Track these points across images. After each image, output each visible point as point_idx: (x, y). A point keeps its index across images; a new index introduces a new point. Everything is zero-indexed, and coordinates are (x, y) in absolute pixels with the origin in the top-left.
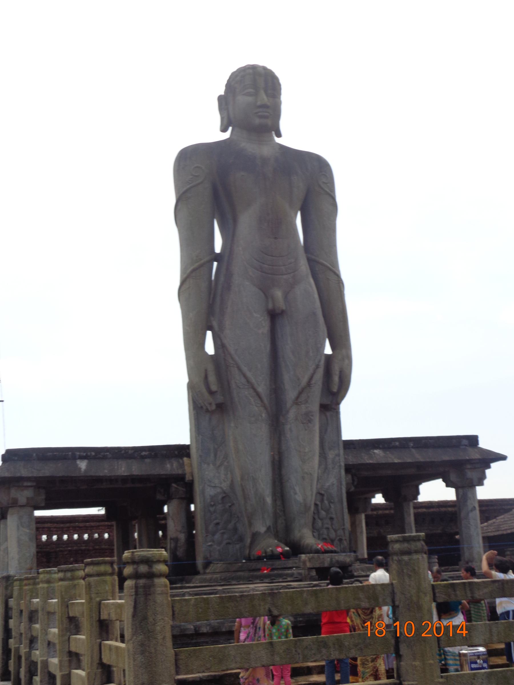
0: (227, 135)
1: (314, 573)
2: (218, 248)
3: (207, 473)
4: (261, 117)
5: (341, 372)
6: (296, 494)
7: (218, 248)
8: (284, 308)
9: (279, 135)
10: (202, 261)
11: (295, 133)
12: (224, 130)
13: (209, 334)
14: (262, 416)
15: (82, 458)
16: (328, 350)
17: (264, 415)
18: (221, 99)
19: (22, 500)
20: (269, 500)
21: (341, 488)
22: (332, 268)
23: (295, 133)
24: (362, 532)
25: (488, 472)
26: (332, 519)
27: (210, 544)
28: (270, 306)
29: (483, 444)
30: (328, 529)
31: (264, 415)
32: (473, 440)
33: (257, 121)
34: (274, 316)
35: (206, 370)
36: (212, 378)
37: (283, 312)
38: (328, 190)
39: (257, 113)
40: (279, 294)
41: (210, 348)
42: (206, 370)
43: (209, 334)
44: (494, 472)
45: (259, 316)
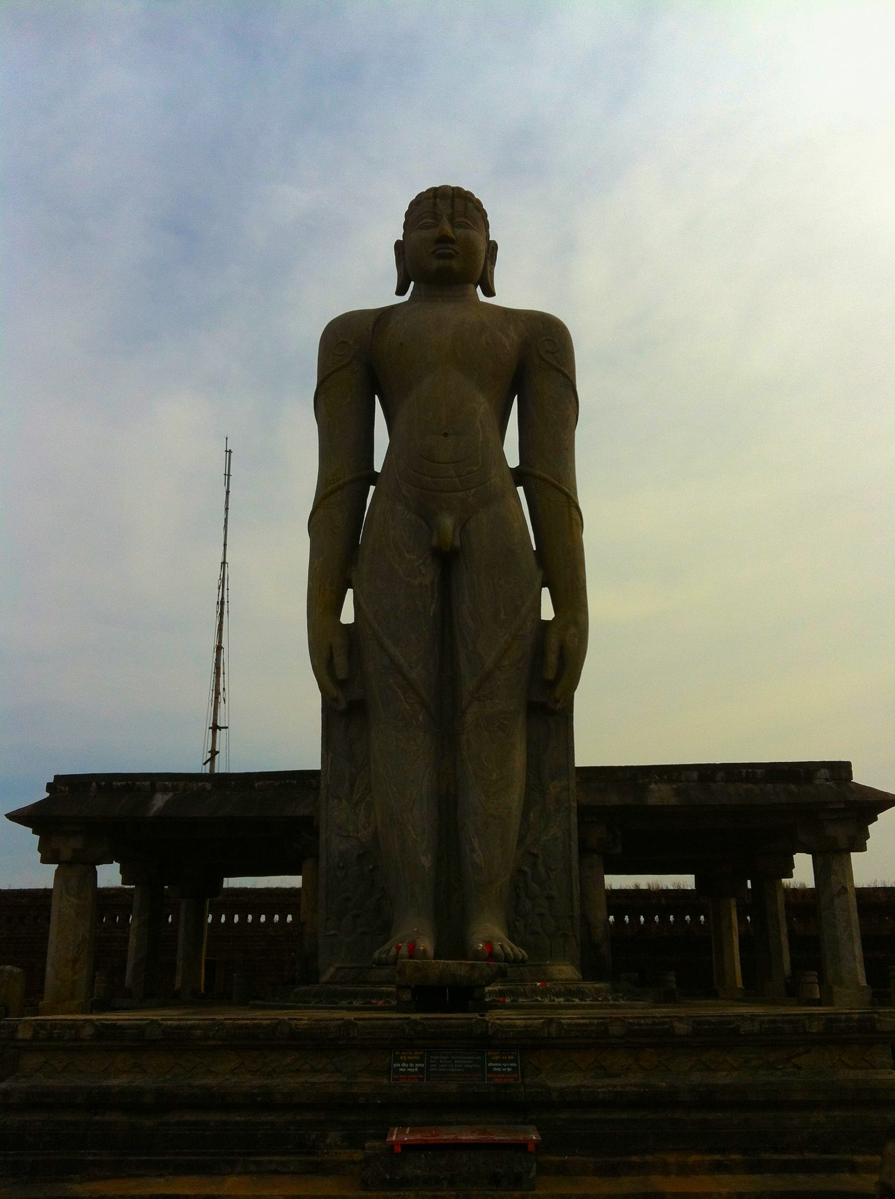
0: (406, 298)
1: (407, 996)
3: (336, 813)
4: (441, 257)
5: (562, 648)
6: (473, 851)
8: (457, 543)
10: (341, 482)
11: (516, 286)
12: (401, 291)
13: (350, 593)
14: (418, 720)
15: (165, 790)
16: (547, 612)
17: (421, 718)
18: (399, 246)
20: (426, 861)
21: (570, 845)
22: (557, 483)
23: (516, 286)
24: (730, 927)
25: (871, 827)
26: (550, 898)
27: (332, 932)
28: (434, 541)
29: (858, 778)
30: (541, 915)
31: (421, 718)
33: (436, 264)
35: (331, 647)
36: (340, 661)
38: (555, 363)
39: (433, 253)
40: (448, 522)
41: (348, 615)
42: (331, 647)
44: (885, 827)
45: (414, 557)
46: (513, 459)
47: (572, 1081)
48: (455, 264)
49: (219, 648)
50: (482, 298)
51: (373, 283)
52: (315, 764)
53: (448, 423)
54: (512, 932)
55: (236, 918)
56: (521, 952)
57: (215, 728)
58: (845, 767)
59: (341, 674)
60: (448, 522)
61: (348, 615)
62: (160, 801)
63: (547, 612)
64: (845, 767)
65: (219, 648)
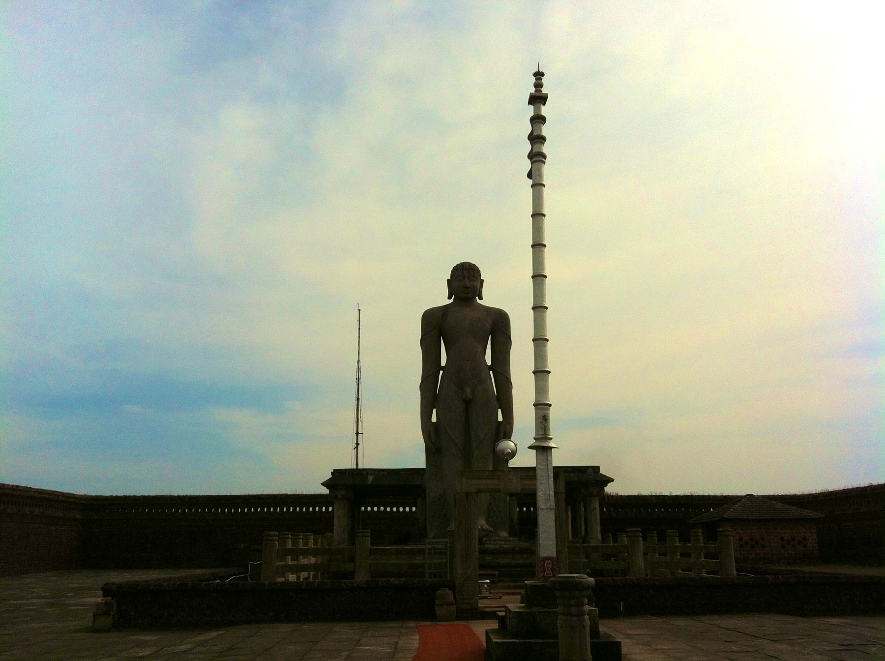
0: (451, 301)
2: (443, 362)
7: (443, 363)
9: (481, 298)
11: (490, 298)
12: (450, 298)
13: (435, 410)
15: (371, 474)
16: (500, 419)
19: (340, 496)
23: (490, 298)
29: (602, 471)
32: (597, 469)
33: (463, 295)
34: (467, 403)
37: (471, 400)
40: (468, 391)
41: (434, 419)
43: (435, 410)
46: (489, 363)
47: (506, 561)
48: (470, 295)
49: (358, 399)
50: (478, 301)
51: (441, 298)
52: (423, 465)
53: (464, 337)
54: (488, 522)
55: (311, 509)
56: (491, 529)
57: (357, 433)
58: (598, 468)
59: (433, 440)
60: (468, 391)
61: (434, 419)
62: (370, 478)
63: (500, 419)
64: (598, 468)
65: (358, 399)
